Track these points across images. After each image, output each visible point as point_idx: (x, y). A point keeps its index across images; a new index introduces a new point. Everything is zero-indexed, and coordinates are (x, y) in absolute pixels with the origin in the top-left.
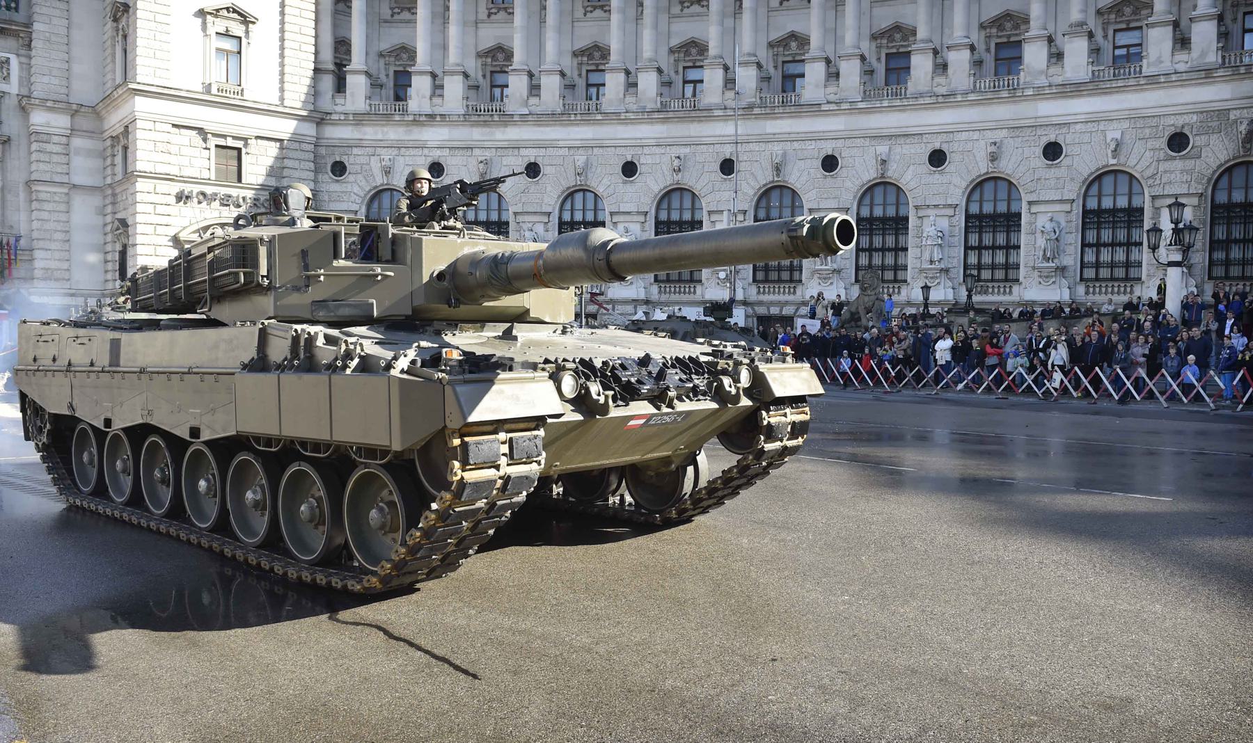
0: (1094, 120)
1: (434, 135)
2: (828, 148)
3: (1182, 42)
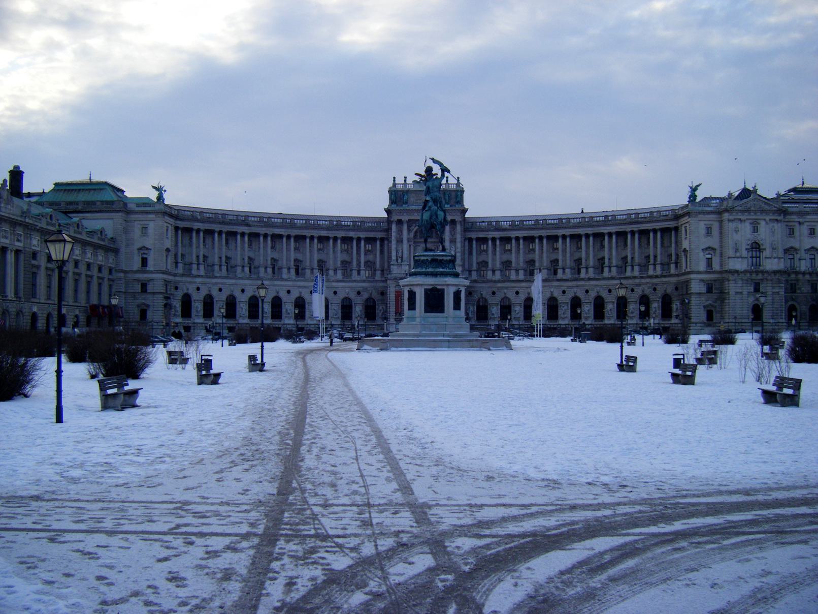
0: (343, 287)
1: (199, 280)
2: (289, 288)
3: (359, 274)
